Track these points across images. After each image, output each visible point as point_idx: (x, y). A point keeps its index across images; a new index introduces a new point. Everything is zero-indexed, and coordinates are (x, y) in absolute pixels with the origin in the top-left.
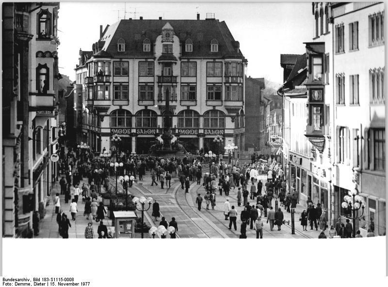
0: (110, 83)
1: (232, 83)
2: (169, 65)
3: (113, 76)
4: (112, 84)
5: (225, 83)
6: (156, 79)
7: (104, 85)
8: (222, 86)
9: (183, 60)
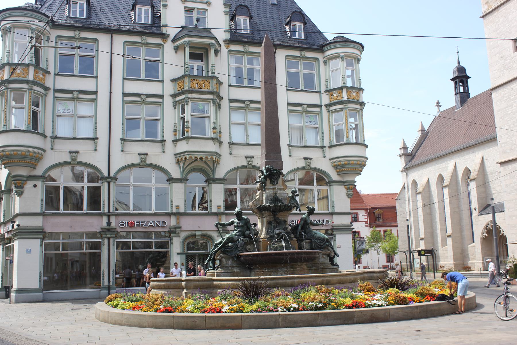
0: (47, 89)
1: (349, 102)
2: (199, 54)
3: (55, 75)
4: (51, 92)
5: (328, 106)
6: (169, 89)
7: (30, 89)
8: (321, 112)
9: (233, 47)
